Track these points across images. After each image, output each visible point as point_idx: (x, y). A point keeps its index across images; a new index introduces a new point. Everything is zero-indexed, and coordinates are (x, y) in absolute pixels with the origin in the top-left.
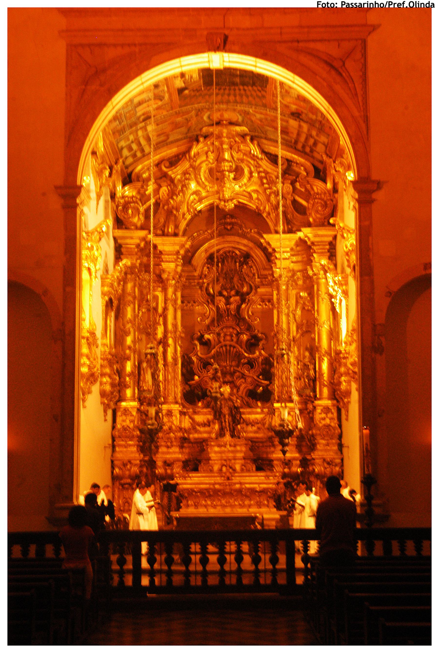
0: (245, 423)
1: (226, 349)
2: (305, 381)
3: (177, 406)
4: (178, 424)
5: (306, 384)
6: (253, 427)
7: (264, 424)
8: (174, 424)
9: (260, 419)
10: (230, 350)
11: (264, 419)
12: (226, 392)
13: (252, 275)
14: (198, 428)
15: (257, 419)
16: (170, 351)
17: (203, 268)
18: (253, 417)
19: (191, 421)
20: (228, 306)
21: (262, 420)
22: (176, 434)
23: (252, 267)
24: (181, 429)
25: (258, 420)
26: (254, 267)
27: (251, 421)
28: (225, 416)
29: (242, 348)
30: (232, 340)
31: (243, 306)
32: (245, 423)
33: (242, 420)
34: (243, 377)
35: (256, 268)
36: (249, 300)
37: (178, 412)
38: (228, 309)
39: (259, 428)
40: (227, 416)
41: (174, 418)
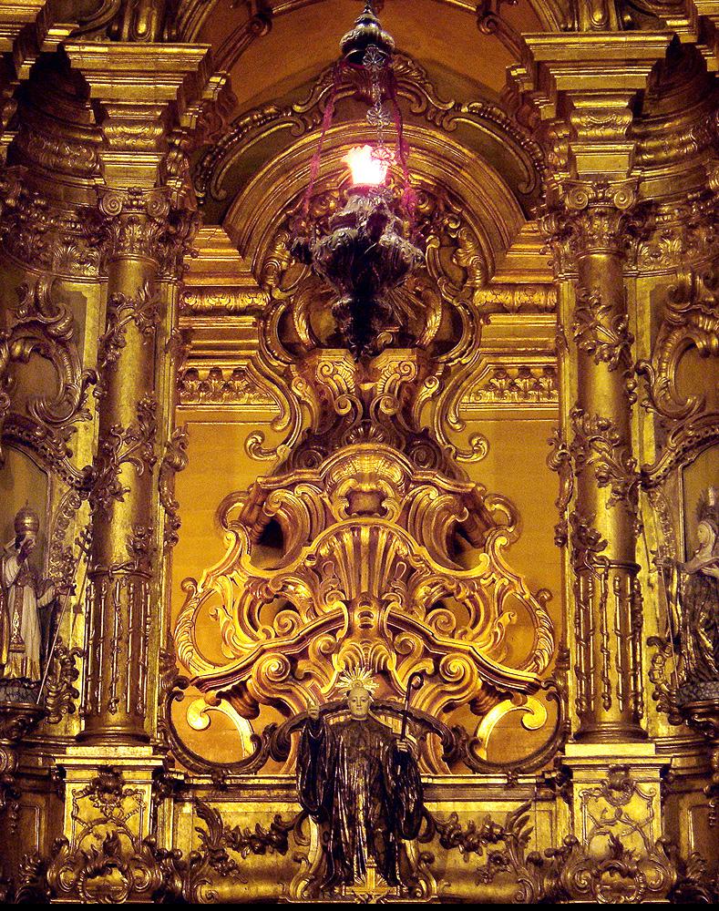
0: (436, 840)
1: (357, 545)
2: (698, 645)
3: (147, 751)
4: (147, 831)
5: (704, 659)
6: (473, 855)
7: (520, 842)
8: (128, 833)
9: (500, 820)
10: (373, 544)
11: (519, 818)
12: (359, 694)
13: (458, 275)
14: (233, 855)
15: (487, 818)
16: (122, 512)
17: (272, 247)
18: (469, 811)
19: (203, 824)
20: (367, 387)
21: (511, 826)
22: (138, 873)
23: (456, 244)
24: (156, 855)
25: (493, 825)
26: (470, 245)
27: (465, 829)
28: (351, 801)
29: (422, 543)
30: (384, 512)
31: (428, 390)
32: (436, 840)
33: (425, 822)
34: (426, 654)
35: (479, 247)
36: (447, 370)
37: (147, 776)
38: (366, 399)
39: (495, 859)
40: (361, 798)
41: (129, 803)
